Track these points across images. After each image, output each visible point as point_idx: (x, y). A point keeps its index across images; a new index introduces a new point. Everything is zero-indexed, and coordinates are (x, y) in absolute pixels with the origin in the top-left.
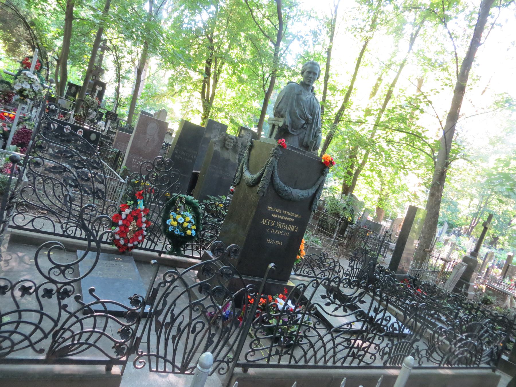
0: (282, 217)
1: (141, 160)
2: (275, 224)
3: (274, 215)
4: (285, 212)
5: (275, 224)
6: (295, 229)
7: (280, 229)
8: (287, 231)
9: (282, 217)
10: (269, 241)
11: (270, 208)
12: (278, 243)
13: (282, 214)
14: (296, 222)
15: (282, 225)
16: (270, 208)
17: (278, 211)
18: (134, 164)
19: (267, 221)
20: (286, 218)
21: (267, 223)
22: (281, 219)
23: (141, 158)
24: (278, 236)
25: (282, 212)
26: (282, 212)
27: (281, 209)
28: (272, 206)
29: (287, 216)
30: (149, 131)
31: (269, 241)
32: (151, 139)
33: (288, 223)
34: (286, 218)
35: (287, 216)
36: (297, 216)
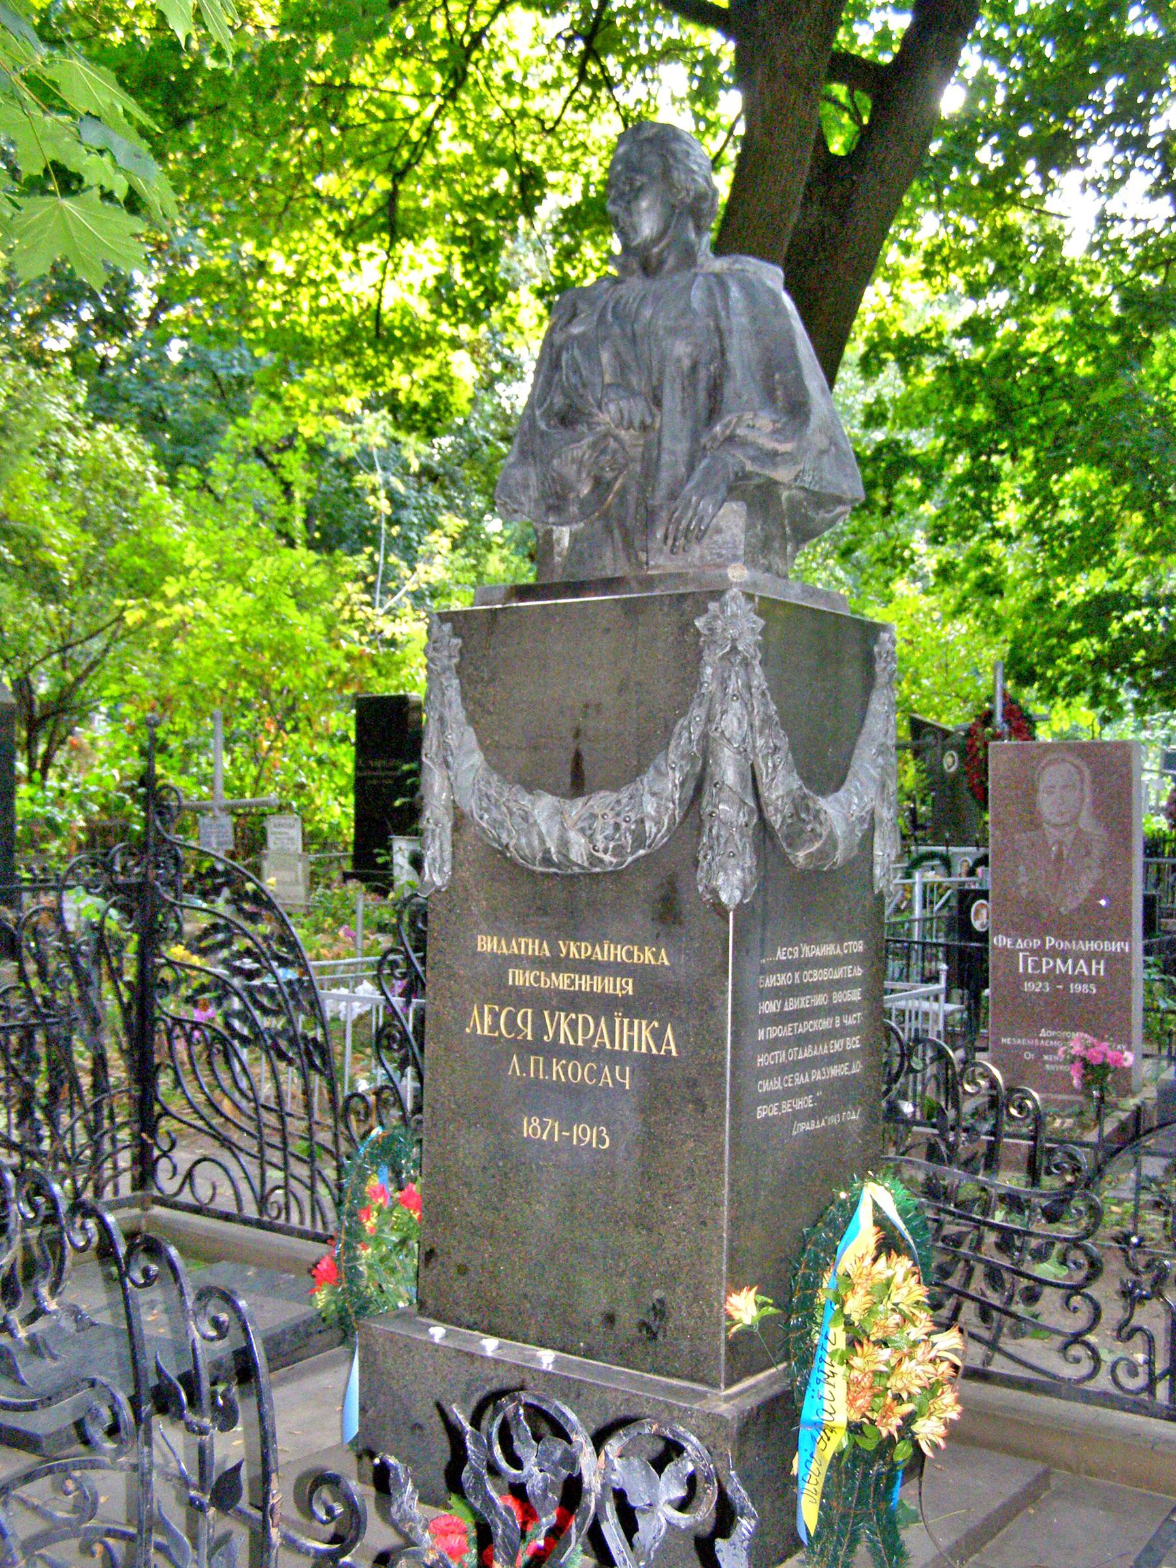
0: (562, 981)
1: (1054, 953)
2: (540, 1029)
3: (520, 978)
4: (574, 950)
5: (540, 1029)
6: (658, 1036)
7: (572, 1053)
8: (615, 1058)
9: (562, 981)
10: (530, 1127)
11: (487, 944)
12: (586, 1135)
13: (556, 964)
14: (651, 997)
15: (573, 1025)
16: (487, 944)
17: (531, 946)
18: (1030, 978)
19: (496, 1016)
20: (584, 983)
21: (495, 1026)
22: (558, 992)
23: (1050, 941)
24: (574, 1091)
25: (554, 948)
26: (554, 948)
27: (542, 934)
28: (496, 930)
29: (589, 967)
30: (1046, 805)
31: (530, 1127)
32: (1069, 839)
33: (604, 1006)
34: (584, 983)
35: (589, 967)
36: (648, 957)
